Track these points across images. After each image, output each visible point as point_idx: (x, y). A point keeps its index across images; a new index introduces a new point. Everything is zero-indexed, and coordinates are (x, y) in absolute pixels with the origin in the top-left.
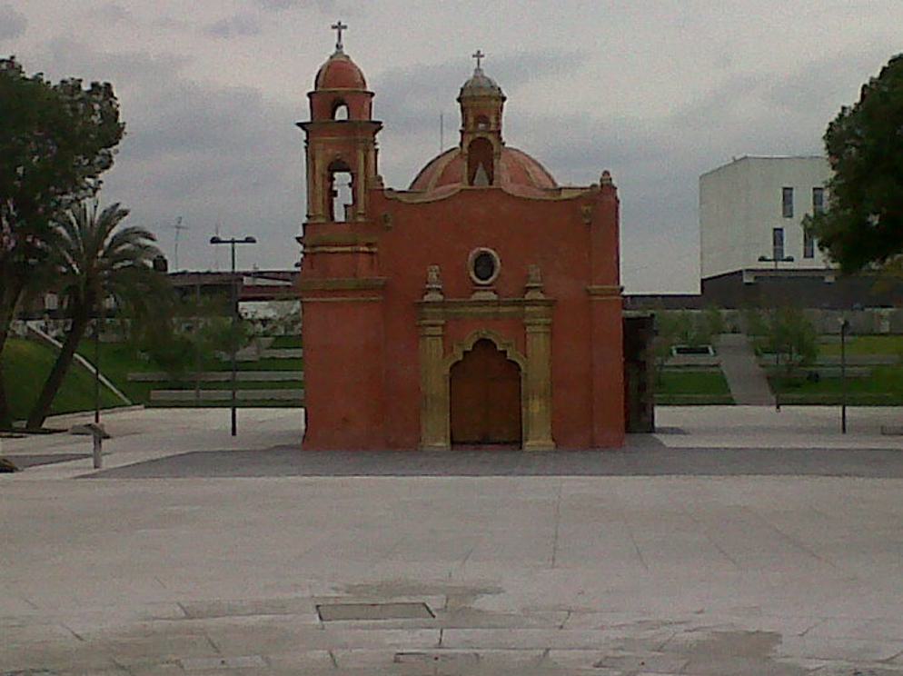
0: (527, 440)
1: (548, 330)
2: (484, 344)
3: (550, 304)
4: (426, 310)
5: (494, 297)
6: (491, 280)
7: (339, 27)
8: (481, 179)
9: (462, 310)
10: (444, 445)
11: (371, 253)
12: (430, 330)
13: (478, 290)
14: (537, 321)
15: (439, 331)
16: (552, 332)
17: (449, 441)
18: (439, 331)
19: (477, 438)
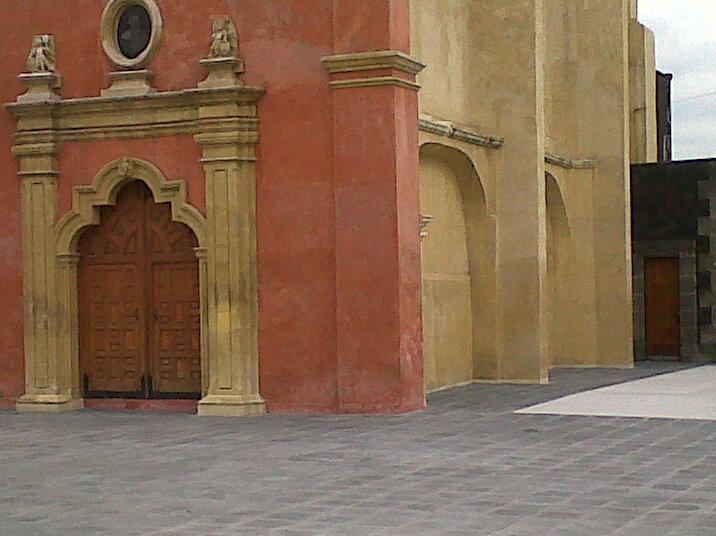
0: (205, 395)
1: (248, 154)
2: (133, 190)
3: (242, 97)
4: (21, 125)
5: (140, 88)
6: (143, 55)
10: (55, 398)
12: (29, 166)
13: (119, 79)
14: (224, 136)
15: (44, 165)
16: (258, 157)
18: (44, 165)
19: (131, 384)
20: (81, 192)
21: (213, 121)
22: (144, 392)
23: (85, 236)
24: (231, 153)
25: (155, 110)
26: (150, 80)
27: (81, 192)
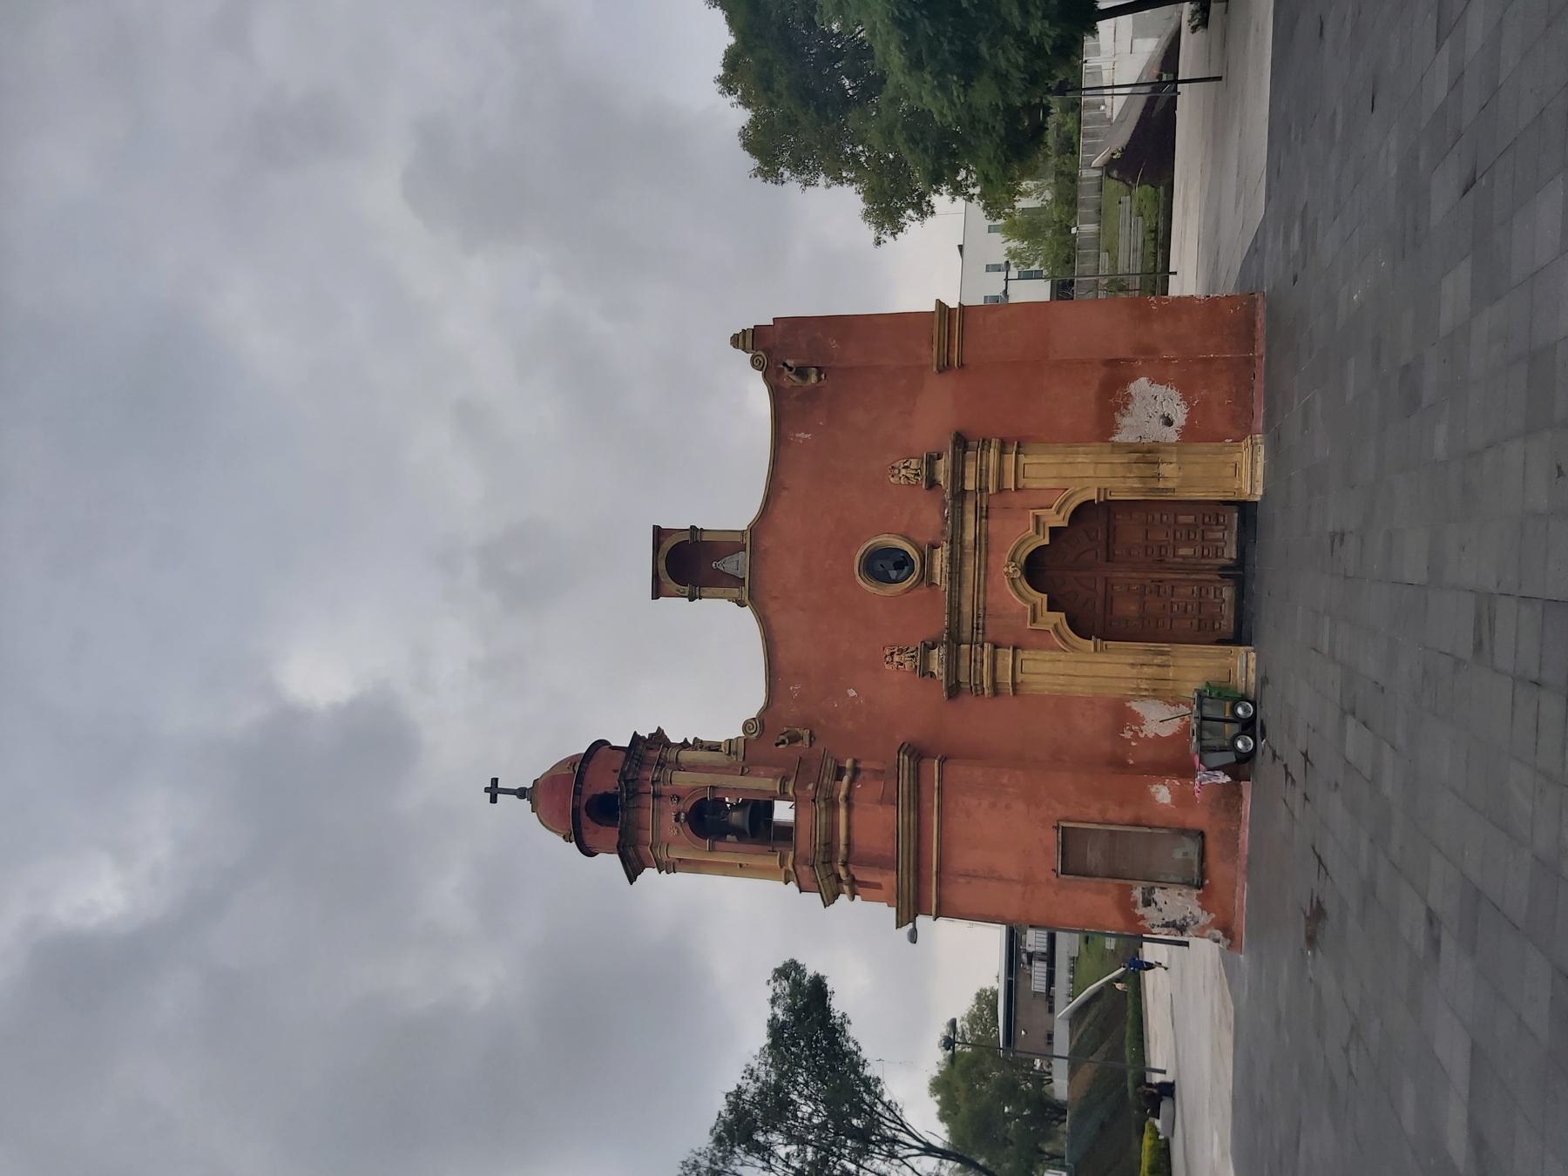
2: (1035, 569)
7: (494, 791)
8: (736, 564)
9: (966, 608)
11: (856, 771)
13: (931, 575)
17: (1233, 648)
18: (1006, 657)
20: (1034, 620)
21: (982, 474)
22: (1239, 573)
23: (1081, 627)
24: (1010, 459)
25: (962, 542)
26: (934, 547)
27: (1034, 620)
